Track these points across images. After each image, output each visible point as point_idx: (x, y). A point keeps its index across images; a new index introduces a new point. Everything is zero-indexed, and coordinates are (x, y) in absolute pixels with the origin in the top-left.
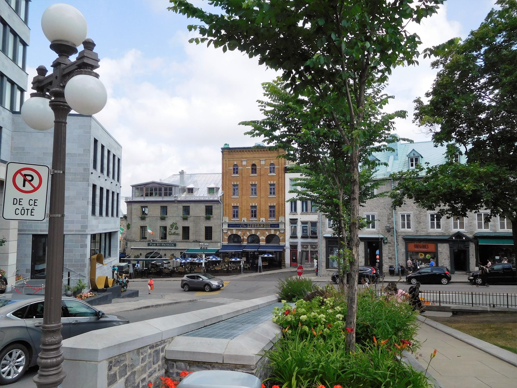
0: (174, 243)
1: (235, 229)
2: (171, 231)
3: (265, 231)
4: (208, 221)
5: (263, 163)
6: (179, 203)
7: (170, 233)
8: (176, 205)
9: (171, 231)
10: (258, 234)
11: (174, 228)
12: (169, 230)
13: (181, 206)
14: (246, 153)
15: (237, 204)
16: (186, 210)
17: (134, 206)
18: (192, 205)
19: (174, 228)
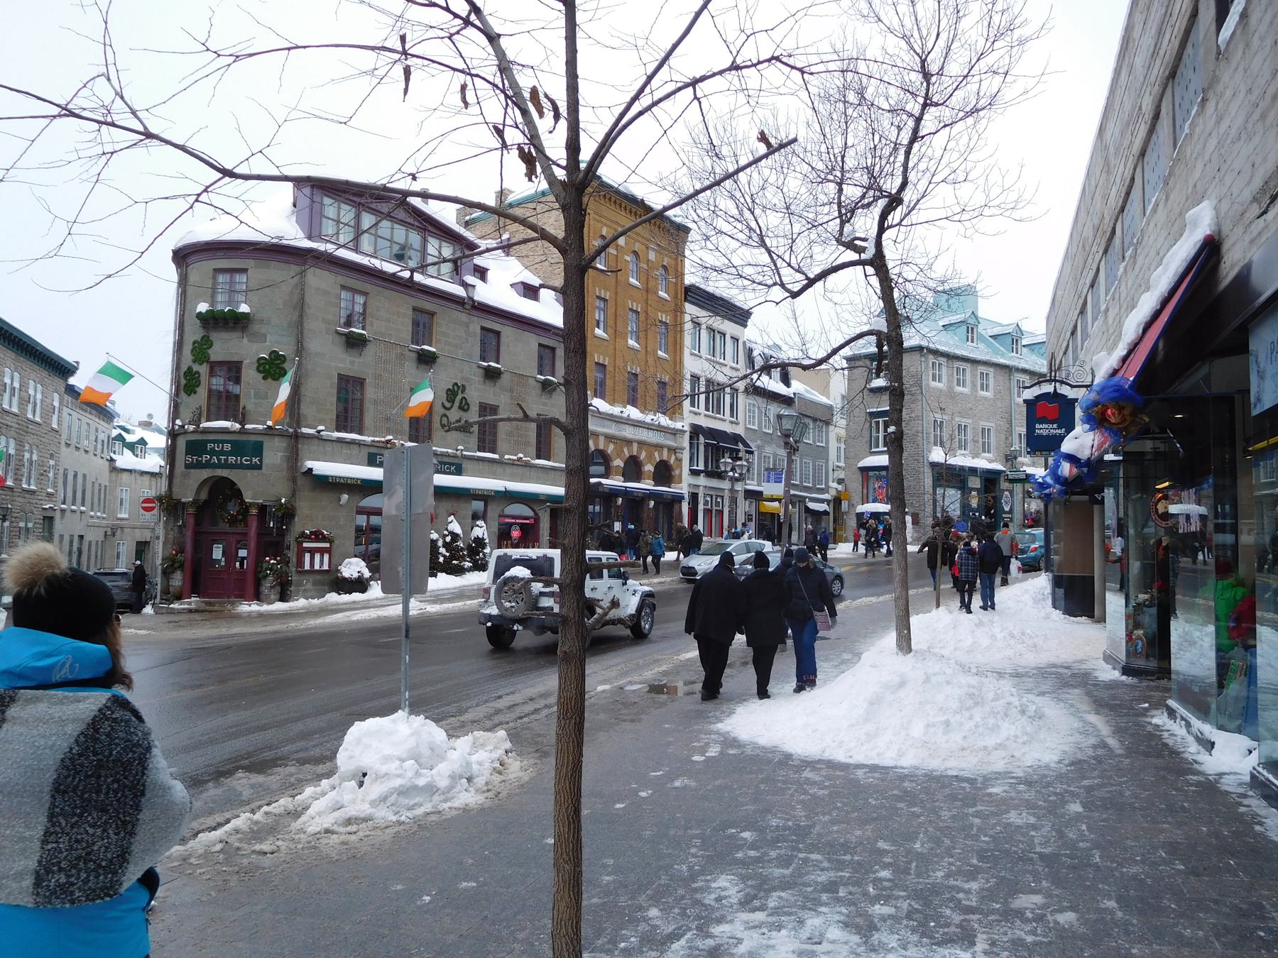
0: (456, 461)
1: (602, 434)
2: (448, 413)
3: (652, 449)
4: (544, 399)
5: (652, 256)
6: (474, 313)
7: (445, 421)
8: (463, 317)
9: (448, 413)
10: (643, 456)
11: (457, 404)
12: (443, 411)
13: (476, 323)
14: (623, 213)
15: (604, 359)
16: (490, 343)
17: (314, 275)
18: (508, 332)
19: (457, 404)
